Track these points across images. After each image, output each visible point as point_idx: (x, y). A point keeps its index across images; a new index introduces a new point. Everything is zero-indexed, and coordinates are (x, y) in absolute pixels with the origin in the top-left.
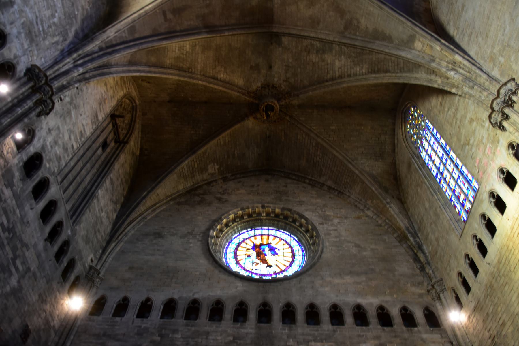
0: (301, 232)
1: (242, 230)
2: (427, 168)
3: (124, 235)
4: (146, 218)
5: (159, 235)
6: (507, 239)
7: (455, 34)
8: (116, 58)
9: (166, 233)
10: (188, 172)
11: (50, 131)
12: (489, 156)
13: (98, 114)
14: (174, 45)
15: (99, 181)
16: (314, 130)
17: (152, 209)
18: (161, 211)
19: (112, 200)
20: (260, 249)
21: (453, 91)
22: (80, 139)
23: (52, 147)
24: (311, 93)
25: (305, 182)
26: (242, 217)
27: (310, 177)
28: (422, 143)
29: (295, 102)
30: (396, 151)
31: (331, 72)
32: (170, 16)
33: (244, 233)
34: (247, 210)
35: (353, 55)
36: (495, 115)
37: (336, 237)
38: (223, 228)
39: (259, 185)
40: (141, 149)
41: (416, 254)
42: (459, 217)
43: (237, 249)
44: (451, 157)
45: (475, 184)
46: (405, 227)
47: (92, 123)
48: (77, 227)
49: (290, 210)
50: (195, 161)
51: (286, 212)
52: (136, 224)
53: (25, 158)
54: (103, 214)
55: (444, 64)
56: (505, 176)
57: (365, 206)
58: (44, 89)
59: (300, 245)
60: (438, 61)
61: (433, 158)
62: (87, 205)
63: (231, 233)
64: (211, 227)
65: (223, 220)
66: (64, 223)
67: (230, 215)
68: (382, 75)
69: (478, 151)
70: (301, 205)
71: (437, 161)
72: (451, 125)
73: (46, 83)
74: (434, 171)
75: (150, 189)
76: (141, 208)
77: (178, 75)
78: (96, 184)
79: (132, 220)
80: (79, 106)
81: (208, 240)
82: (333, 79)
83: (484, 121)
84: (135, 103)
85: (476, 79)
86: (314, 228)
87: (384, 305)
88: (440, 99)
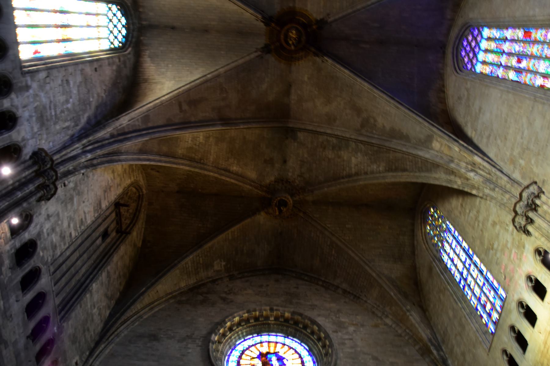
0: (312, 340)
1: (247, 335)
2: (449, 273)
3: (116, 336)
4: (142, 318)
5: (154, 337)
6: (540, 355)
7: (473, 136)
8: (127, 145)
9: (162, 336)
10: (192, 268)
11: (48, 217)
12: (515, 262)
13: (102, 201)
14: (187, 135)
15: (94, 273)
16: (329, 227)
17: (149, 307)
18: (160, 310)
19: (106, 295)
20: (267, 358)
21: (474, 192)
22: (80, 227)
23: (48, 235)
24: (326, 189)
25: (317, 284)
26: (247, 321)
27: (323, 279)
28: (443, 245)
29: (310, 198)
30: (416, 253)
31: (347, 169)
32: (185, 107)
33: (249, 339)
34: (254, 313)
35: (370, 153)
36: (519, 219)
37: (352, 347)
38: (227, 332)
39: (268, 285)
40: (144, 241)
42: (486, 328)
43: (240, 357)
44: (475, 262)
45: (501, 292)
46: (428, 338)
47: (95, 211)
48: (65, 324)
49: (301, 315)
50: (200, 256)
51: (297, 317)
52: (130, 324)
53: (18, 244)
54: (95, 311)
55: (463, 165)
56: (533, 285)
57: (383, 313)
58: (49, 174)
59: (311, 356)
60: (457, 162)
61: (455, 262)
62: (79, 300)
63: (235, 338)
64: (213, 331)
65: (226, 323)
66: (51, 319)
67: (235, 317)
68: (400, 174)
70: (313, 309)
71: (460, 266)
72: (473, 228)
73: (52, 168)
74: (457, 276)
75: (149, 285)
76: (138, 306)
77: (189, 166)
78: (91, 277)
79: (126, 319)
80: (83, 193)
81: (208, 346)
82: (349, 176)
83: (507, 225)
84: (142, 192)
85: (497, 181)
86: (327, 336)
88: (461, 200)
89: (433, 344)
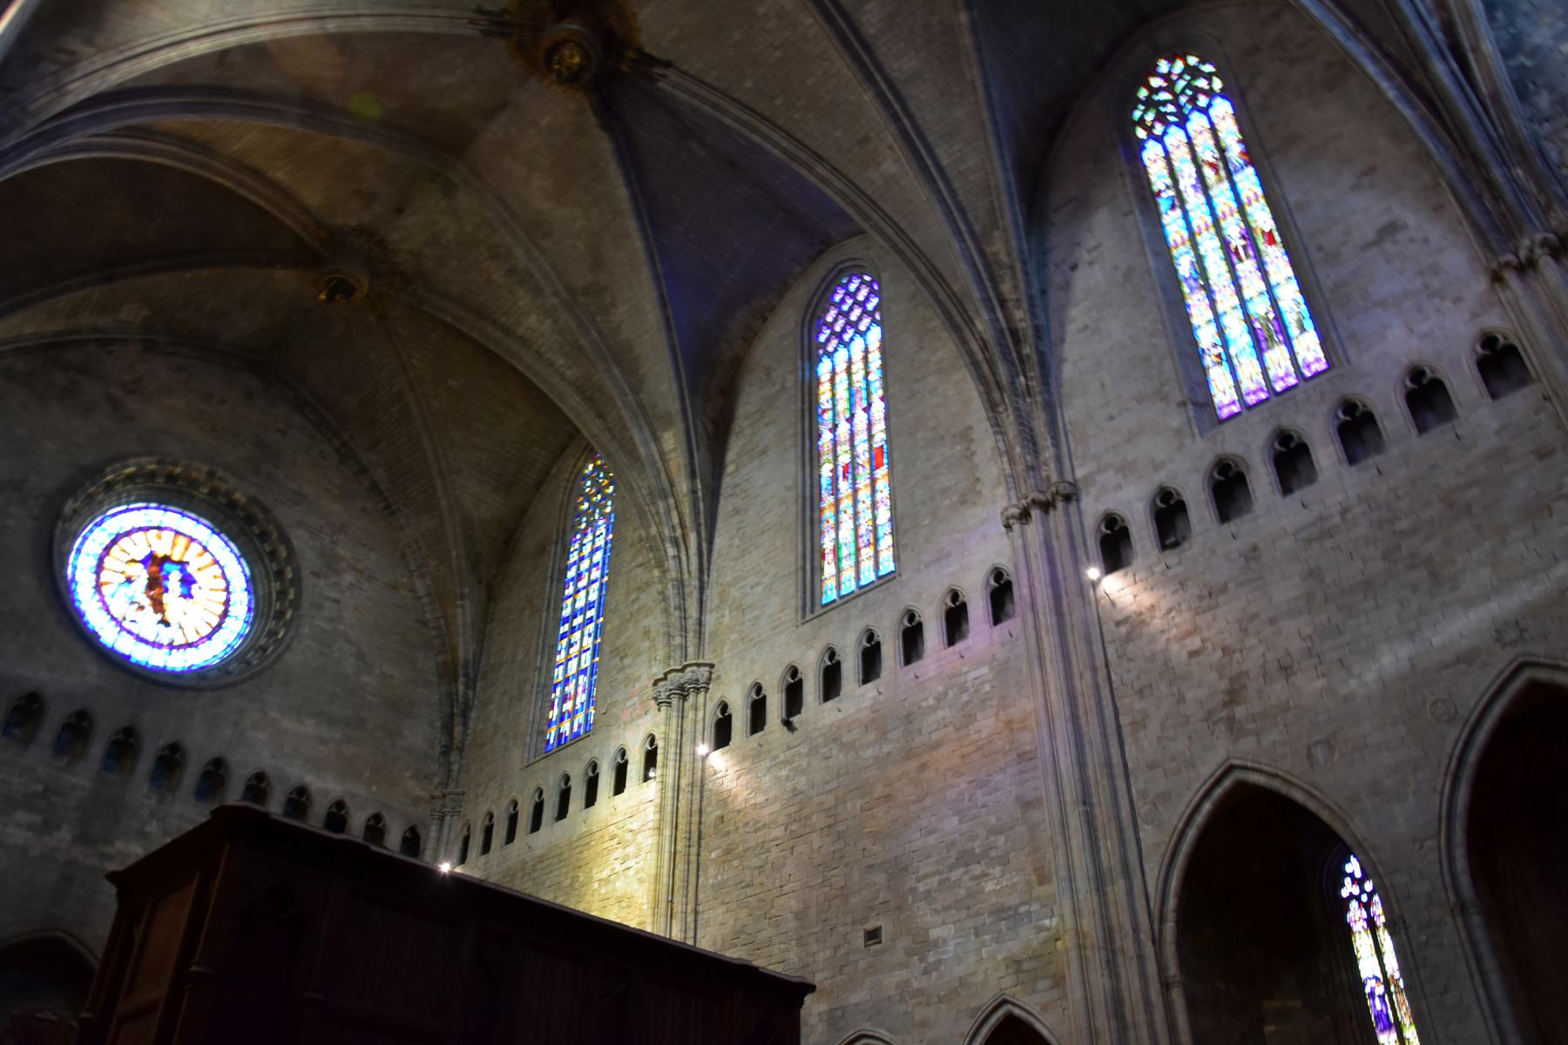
20: (161, 569)
26: (152, 476)
37: (331, 620)
39: (223, 401)
41: (452, 715)
42: (546, 727)
43: (107, 550)
49: (266, 510)
51: (255, 510)
59: (249, 593)
69: (622, 686)
72: (628, 594)
77: (176, 157)
82: (508, 331)
86: (297, 582)
87: (348, 802)
89: (466, 675)
